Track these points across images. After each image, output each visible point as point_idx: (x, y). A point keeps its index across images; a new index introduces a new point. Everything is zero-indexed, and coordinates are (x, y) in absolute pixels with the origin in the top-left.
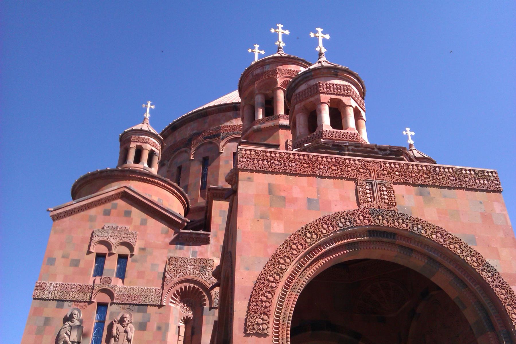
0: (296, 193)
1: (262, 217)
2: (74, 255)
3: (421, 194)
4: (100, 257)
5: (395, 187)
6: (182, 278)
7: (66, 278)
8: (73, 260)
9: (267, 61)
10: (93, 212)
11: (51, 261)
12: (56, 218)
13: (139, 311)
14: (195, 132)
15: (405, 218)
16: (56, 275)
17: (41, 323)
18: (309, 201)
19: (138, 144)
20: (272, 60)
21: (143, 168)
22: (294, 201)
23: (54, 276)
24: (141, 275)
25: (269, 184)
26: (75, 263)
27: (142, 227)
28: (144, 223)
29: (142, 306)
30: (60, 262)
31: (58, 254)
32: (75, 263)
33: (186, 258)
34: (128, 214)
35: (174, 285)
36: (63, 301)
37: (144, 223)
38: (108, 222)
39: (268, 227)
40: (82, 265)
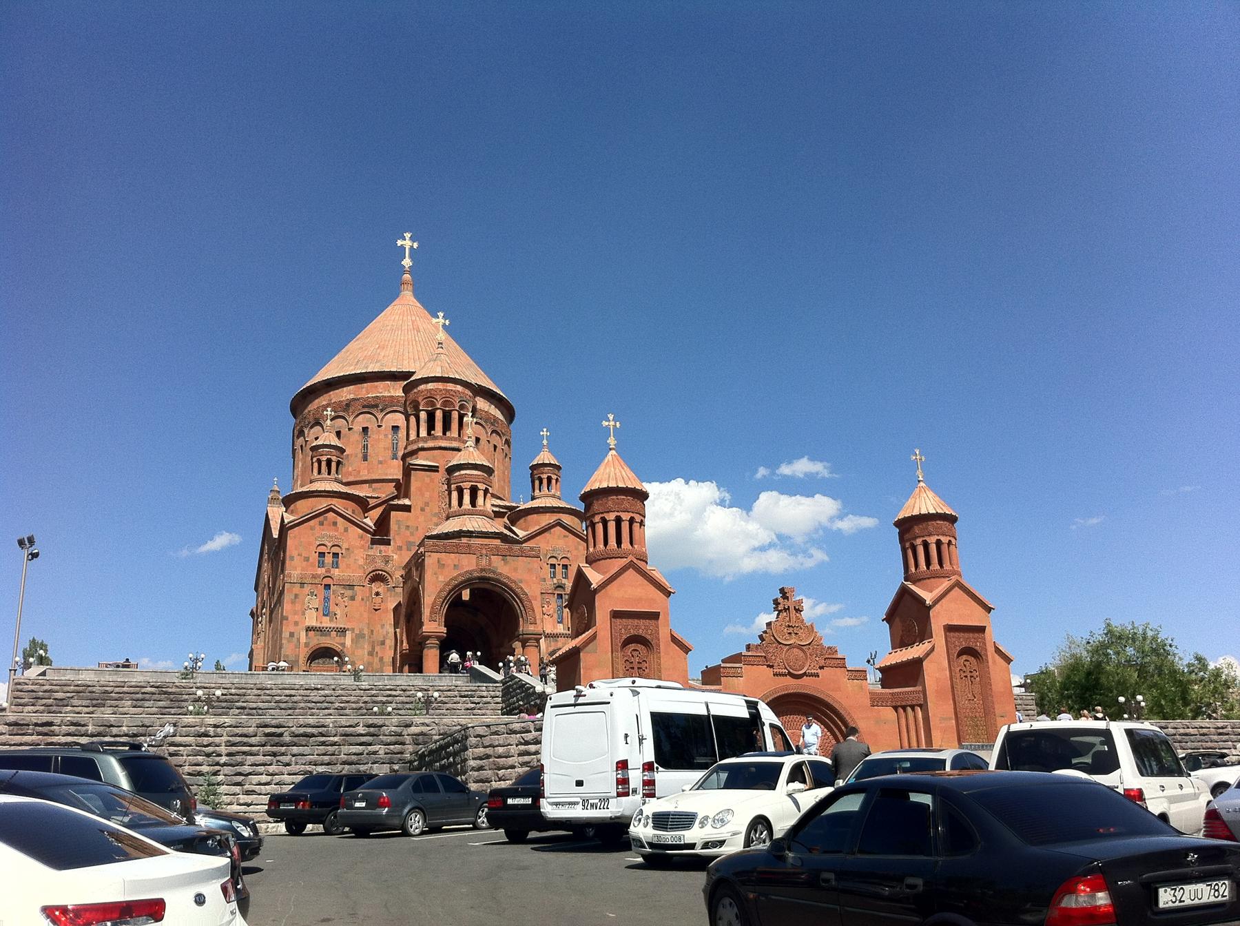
0: (450, 562)
3: (503, 560)
4: (322, 555)
5: (492, 557)
8: (305, 557)
10: (312, 523)
14: (352, 396)
15: (494, 572)
16: (296, 568)
17: (293, 598)
18: (455, 565)
19: (329, 457)
22: (448, 565)
23: (295, 569)
24: (348, 566)
26: (307, 559)
28: (346, 530)
29: (351, 587)
32: (307, 559)
34: (335, 524)
35: (370, 573)
37: (346, 530)
38: (323, 530)
39: (437, 578)
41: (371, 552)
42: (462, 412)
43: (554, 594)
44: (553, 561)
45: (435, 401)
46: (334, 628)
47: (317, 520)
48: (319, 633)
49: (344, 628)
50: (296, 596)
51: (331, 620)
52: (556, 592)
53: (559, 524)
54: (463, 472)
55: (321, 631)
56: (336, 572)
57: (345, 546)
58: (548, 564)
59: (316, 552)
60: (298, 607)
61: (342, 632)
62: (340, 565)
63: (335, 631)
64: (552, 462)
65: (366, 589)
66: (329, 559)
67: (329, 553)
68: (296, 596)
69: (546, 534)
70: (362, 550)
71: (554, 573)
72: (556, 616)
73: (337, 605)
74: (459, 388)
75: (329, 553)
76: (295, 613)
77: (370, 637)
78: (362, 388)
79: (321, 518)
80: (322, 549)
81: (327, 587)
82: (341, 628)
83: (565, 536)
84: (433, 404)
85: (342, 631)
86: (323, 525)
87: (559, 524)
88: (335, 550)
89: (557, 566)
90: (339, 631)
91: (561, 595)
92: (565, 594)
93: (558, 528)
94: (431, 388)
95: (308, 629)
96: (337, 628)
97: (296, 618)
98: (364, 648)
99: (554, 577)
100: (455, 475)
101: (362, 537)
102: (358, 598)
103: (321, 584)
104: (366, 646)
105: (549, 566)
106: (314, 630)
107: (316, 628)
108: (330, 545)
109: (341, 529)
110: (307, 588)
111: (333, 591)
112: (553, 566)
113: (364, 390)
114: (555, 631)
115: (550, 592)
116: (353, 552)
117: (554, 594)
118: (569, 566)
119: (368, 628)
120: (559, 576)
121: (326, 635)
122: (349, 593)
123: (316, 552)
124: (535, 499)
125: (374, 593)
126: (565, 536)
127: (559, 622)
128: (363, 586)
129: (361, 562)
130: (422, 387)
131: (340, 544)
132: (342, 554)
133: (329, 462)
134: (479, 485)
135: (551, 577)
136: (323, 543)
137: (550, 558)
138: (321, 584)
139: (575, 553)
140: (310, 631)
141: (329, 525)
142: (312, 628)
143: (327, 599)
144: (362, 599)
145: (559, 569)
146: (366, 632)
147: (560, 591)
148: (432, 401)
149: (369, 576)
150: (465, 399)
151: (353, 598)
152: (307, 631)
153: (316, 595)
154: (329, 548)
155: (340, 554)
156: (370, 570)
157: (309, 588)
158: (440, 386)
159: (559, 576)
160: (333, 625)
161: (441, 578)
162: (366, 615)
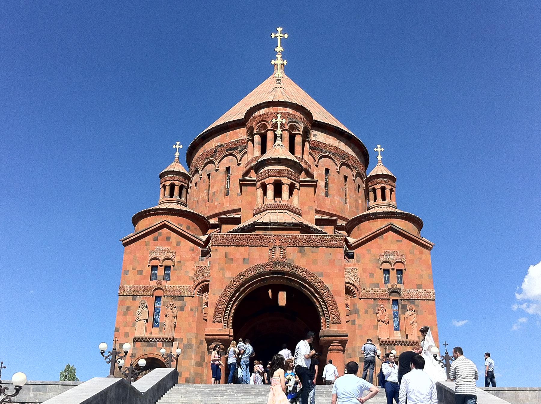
2: (139, 268)
4: (154, 268)
6: (203, 279)
7: (136, 281)
9: (262, 105)
11: (126, 272)
12: (125, 245)
13: (179, 300)
20: (266, 104)
21: (176, 200)
23: (129, 282)
24: (179, 278)
26: (140, 273)
27: (178, 247)
28: (178, 244)
29: (181, 297)
30: (131, 273)
31: (129, 268)
32: (140, 273)
33: (206, 266)
34: (168, 239)
35: (199, 284)
36: (136, 296)
37: (178, 244)
38: (157, 245)
40: (144, 274)
41: (201, 264)
42: (293, 132)
43: (389, 299)
44: (386, 266)
45: (267, 124)
46: (160, 339)
47: (151, 237)
48: (146, 343)
49: (170, 339)
50: (128, 308)
51: (160, 331)
52: (392, 298)
53: (391, 229)
54: (266, 168)
55: (148, 341)
56: (167, 284)
57: (177, 259)
58: (381, 269)
59: (149, 266)
60: (129, 319)
61: (169, 342)
62: (171, 277)
63: (162, 341)
64: (385, 173)
65: (195, 300)
66: (160, 272)
67: (161, 266)
68: (128, 308)
69: (379, 240)
70: (193, 262)
71: (388, 278)
72: (392, 323)
73: (166, 316)
74: (289, 111)
75: (161, 266)
76: (127, 325)
77: (199, 348)
78: (227, 136)
79: (156, 234)
80: (155, 263)
81: (158, 298)
82: (167, 339)
83: (398, 241)
84: (265, 126)
85: (168, 341)
87: (391, 229)
88: (168, 263)
89: (391, 270)
90: (165, 341)
91: (397, 300)
92: (401, 300)
93: (391, 233)
94: (264, 113)
95: (136, 340)
96: (163, 339)
97: (127, 329)
98: (191, 359)
99: (389, 282)
100: (260, 172)
101: (193, 250)
102: (188, 308)
103: (153, 296)
104: (193, 357)
105: (382, 270)
106: (141, 341)
107: (142, 338)
108: (162, 258)
109: (174, 243)
110: (139, 300)
111: (163, 302)
112: (387, 271)
113: (228, 137)
114: (392, 339)
115: (384, 297)
116: (184, 264)
117: (389, 299)
118: (404, 271)
119: (196, 338)
120: (393, 280)
121: (152, 346)
122: (178, 303)
123: (149, 266)
124: (370, 209)
125: (204, 302)
126: (398, 241)
127: (395, 330)
128: (193, 297)
129: (192, 273)
130: (257, 114)
131: (173, 257)
132: (174, 266)
133: (172, 186)
134: (284, 180)
135: (385, 283)
136: (156, 256)
137: (381, 264)
138: (153, 296)
139: (410, 257)
140: (137, 341)
141: (163, 240)
142: (139, 338)
143: (156, 311)
144: (191, 310)
145: (393, 274)
146: (194, 342)
147: (395, 296)
148: (264, 124)
149: (199, 287)
150: (295, 120)
151: (182, 309)
152: (134, 341)
153: (146, 307)
154: (161, 261)
155: (172, 267)
156: (200, 281)
157: (141, 300)
158: (271, 110)
159: (393, 280)
160: (161, 335)
162: (194, 325)
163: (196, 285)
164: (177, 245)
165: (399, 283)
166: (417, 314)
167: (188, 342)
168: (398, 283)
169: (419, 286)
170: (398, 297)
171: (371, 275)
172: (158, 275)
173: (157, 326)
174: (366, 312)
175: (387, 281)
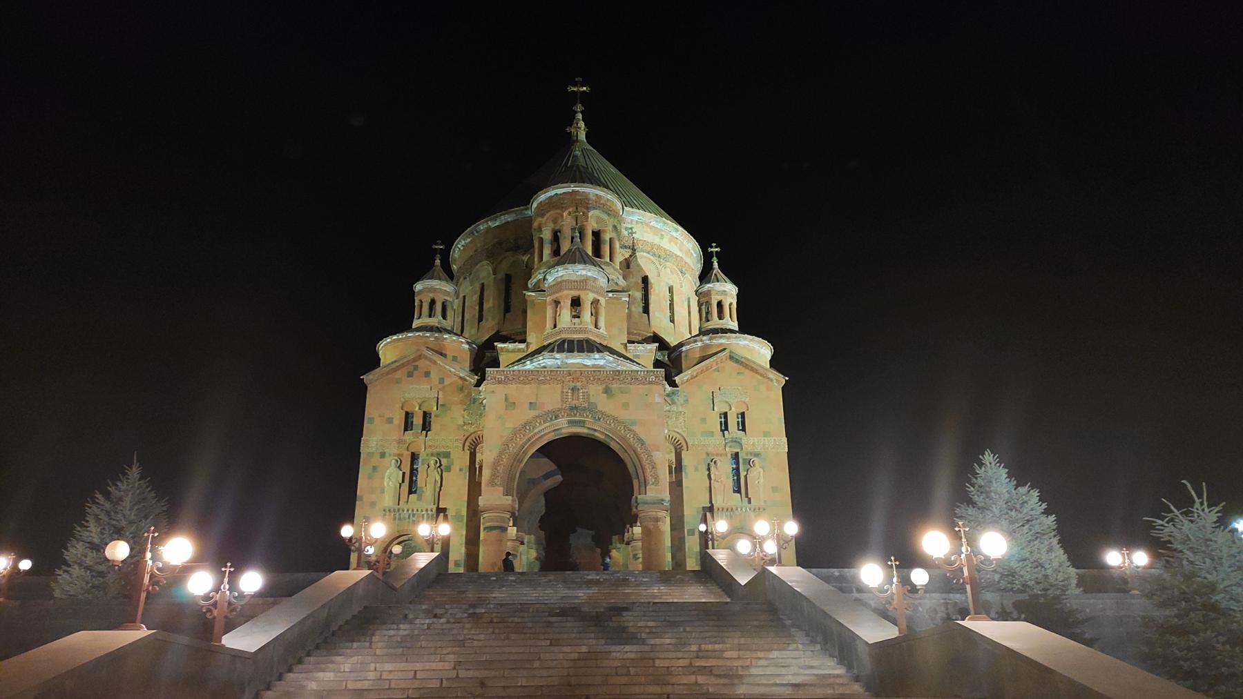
1: (500, 418)
18: (531, 403)
25: (506, 395)
34: (427, 374)
50: (375, 468)
83: (738, 373)
86: (412, 376)
111: (423, 460)
116: (450, 409)
144: (461, 470)
161: (510, 425)
163: (466, 436)
164: (440, 383)
165: (740, 430)
166: (764, 471)
167: (457, 513)
168: (739, 430)
169: (766, 434)
170: (737, 448)
171: (704, 420)
172: (414, 423)
173: (415, 492)
174: (696, 469)
175: (723, 428)
